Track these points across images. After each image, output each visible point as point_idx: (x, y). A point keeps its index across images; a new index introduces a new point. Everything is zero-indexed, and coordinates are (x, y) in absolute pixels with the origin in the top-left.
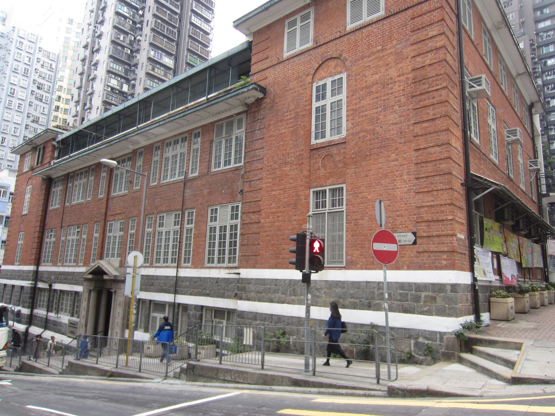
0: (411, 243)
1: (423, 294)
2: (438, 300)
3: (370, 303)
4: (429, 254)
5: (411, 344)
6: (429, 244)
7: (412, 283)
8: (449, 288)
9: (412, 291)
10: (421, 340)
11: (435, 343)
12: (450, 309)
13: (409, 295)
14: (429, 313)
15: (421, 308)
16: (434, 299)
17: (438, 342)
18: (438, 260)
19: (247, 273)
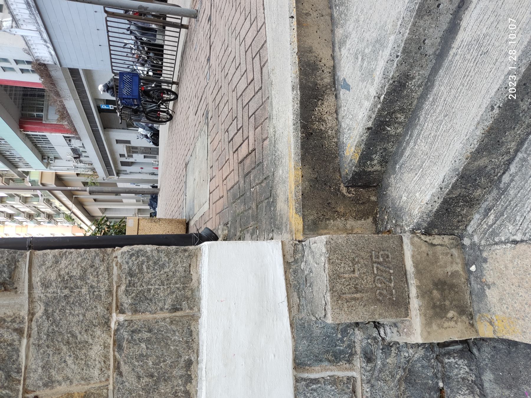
12: (141, 300)
17: (357, 370)
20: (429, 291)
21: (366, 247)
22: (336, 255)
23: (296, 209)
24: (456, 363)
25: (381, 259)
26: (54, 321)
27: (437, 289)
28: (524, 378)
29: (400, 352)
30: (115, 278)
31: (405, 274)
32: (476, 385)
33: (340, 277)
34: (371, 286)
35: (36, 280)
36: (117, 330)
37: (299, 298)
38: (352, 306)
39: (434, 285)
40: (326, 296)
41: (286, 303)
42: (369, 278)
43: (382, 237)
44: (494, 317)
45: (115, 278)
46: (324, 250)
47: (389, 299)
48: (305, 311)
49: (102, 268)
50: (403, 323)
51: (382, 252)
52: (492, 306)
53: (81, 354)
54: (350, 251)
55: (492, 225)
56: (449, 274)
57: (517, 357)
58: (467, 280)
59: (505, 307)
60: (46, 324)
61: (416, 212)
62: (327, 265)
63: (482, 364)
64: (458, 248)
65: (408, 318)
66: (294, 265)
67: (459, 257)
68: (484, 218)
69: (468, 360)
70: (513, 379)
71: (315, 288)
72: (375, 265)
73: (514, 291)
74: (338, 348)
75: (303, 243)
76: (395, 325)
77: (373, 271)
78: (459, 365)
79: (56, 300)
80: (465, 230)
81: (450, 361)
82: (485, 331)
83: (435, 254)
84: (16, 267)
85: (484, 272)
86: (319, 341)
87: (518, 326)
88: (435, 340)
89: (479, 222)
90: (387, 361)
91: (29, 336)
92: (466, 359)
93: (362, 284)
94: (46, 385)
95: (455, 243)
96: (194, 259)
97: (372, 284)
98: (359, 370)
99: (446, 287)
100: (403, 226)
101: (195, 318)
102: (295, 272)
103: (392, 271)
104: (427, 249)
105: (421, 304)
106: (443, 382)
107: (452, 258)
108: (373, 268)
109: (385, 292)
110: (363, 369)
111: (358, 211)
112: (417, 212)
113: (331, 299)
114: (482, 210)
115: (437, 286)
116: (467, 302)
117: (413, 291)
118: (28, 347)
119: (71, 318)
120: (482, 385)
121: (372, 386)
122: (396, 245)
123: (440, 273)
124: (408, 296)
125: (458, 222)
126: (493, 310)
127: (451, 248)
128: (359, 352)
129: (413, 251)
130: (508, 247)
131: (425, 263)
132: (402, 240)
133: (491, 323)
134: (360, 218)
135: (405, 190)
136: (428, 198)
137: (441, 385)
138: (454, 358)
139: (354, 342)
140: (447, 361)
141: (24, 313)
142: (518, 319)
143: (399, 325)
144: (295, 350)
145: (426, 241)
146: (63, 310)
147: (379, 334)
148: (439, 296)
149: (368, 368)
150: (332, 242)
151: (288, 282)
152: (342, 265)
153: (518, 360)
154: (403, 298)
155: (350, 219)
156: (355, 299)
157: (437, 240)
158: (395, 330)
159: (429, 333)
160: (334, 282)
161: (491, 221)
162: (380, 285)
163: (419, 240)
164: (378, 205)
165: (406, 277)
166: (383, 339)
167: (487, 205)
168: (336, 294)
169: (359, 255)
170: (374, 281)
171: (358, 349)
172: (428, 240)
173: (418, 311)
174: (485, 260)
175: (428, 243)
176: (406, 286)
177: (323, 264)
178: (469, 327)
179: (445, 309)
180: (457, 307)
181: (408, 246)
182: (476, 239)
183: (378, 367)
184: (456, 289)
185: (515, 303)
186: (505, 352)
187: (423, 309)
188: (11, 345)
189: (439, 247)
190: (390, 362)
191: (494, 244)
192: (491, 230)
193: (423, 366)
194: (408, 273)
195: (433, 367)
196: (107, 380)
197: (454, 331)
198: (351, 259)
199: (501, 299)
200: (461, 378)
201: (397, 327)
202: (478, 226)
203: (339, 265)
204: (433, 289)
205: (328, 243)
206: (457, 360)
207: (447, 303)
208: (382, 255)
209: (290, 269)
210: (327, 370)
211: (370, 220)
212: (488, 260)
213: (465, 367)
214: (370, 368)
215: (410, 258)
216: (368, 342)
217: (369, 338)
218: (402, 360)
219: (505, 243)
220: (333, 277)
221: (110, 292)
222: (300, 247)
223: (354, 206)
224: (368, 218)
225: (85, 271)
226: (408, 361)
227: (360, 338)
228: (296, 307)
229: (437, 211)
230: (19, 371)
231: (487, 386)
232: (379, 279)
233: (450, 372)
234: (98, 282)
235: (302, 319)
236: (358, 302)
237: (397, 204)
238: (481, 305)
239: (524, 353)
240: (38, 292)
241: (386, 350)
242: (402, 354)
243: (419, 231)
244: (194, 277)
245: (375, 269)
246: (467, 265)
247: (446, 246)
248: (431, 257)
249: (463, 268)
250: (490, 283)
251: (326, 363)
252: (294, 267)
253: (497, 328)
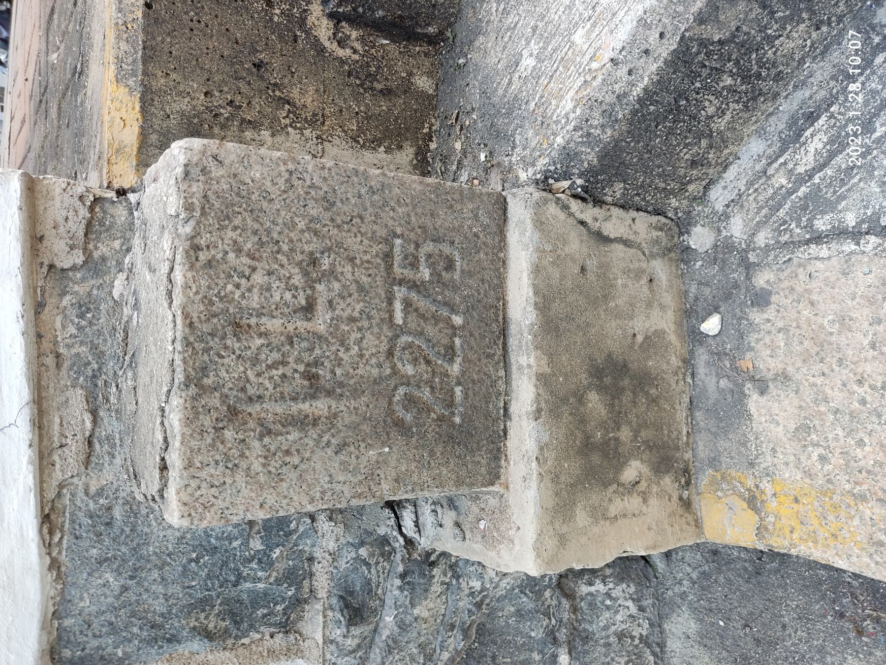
20: (574, 394)
21: (369, 218)
22: (230, 234)
23: (119, 61)
24: (608, 595)
25: (425, 273)
27: (601, 389)
28: (793, 644)
29: (458, 578)
31: (504, 332)
32: (649, 646)
33: (238, 328)
34: (375, 372)
37: (94, 413)
38: (287, 452)
39: (591, 375)
40: (167, 409)
42: (370, 340)
43: (436, 188)
44: (766, 485)
47: (441, 419)
48: (118, 461)
50: (477, 498)
51: (429, 247)
52: (766, 448)
54: (301, 225)
55: (810, 175)
56: (640, 338)
57: (779, 586)
58: (685, 361)
59: (815, 457)
61: (567, 104)
62: (178, 277)
63: (670, 593)
64: (670, 259)
65: (495, 488)
66: (83, 279)
67: (671, 287)
68: (782, 151)
69: (639, 584)
70: (758, 641)
71: (142, 371)
72: (400, 292)
73: (863, 402)
74: (248, 585)
75: (132, 197)
76: (452, 504)
77: (391, 313)
78: (615, 600)
80: (702, 198)
81: (592, 589)
82: (728, 524)
83: (604, 267)
85: (753, 337)
86: (174, 571)
87: (856, 522)
88: (579, 561)
89: (758, 167)
90: (416, 612)
92: (633, 580)
93: (339, 362)
95: (664, 241)
97: (380, 366)
98: (316, 653)
99: (626, 382)
100: (510, 170)
103: (458, 320)
104: (585, 250)
105: (546, 438)
106: (570, 653)
107: (651, 290)
108: (390, 302)
109: (426, 394)
110: (333, 647)
111: (368, 118)
112: (570, 105)
113: (188, 421)
114: (778, 124)
115: (600, 378)
116: (680, 433)
117: (524, 394)
120: (662, 645)
122: (485, 228)
123: (613, 334)
124: (506, 409)
125: (694, 164)
126: (766, 461)
127: (653, 256)
128: (322, 594)
129: (540, 251)
130: (870, 247)
131: (571, 298)
132: (505, 210)
133: (753, 502)
134: (374, 144)
135: (535, 29)
136: (623, 34)
138: (604, 582)
139: (311, 559)
140: (584, 589)
142: (863, 498)
143: (464, 503)
144: (56, 614)
145: (582, 223)
147: (400, 527)
148: (604, 412)
149: (351, 643)
150: (217, 172)
151: (46, 345)
152: (259, 278)
153: (780, 593)
154: (487, 415)
155: (336, 141)
156: (302, 422)
157: (616, 223)
158: (448, 518)
159: (563, 540)
160: (207, 350)
161: (810, 158)
162: (409, 370)
163: (562, 216)
164: (435, 108)
165: (505, 344)
166: (409, 543)
167: (804, 102)
168: (214, 401)
169: (339, 245)
170: (390, 354)
171: (322, 583)
172: (589, 221)
173: (534, 464)
174: (761, 299)
175: (589, 230)
176: (502, 373)
177: (165, 268)
178: (680, 511)
179: (617, 454)
180: (650, 448)
181: (523, 233)
182: (737, 228)
183: (385, 633)
184: (653, 391)
185: (861, 443)
186: (745, 569)
187: (550, 455)
189: (620, 247)
190: (425, 614)
191: (808, 242)
192: (803, 190)
193: (520, 614)
194: (513, 329)
195: (547, 615)
197: (640, 525)
198: (299, 257)
199: (804, 429)
200: (615, 633)
201: (456, 508)
202: (750, 184)
203: (242, 275)
204: (589, 388)
205: (195, 172)
206: (611, 585)
207: (625, 434)
208: (429, 256)
209: (63, 294)
211: (407, 155)
212: (774, 299)
213: (630, 603)
214: (357, 641)
215: (525, 276)
216: (358, 558)
217: (362, 544)
218: (461, 604)
219: (856, 235)
220: (206, 328)
223: (357, 97)
224: (400, 147)
226: (479, 605)
227: (332, 545)
228: (74, 449)
229: (648, 96)
231: (674, 647)
232: (410, 345)
233: (591, 623)
235: (100, 492)
236: (313, 433)
237: (500, 92)
238: (722, 444)
239: (805, 578)
241: (415, 578)
242: (464, 585)
243: (566, 184)
245: (398, 306)
246: (690, 315)
247: (639, 247)
248: (594, 279)
249: (679, 324)
250: (770, 375)
251: (196, 645)
252: (81, 289)
253: (771, 519)
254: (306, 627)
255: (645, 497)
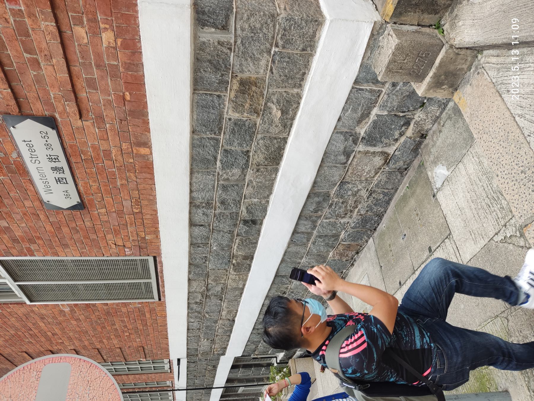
0: (52, 133)
1: (230, 113)
2: (254, 76)
3: (245, 222)
4: (80, 84)
5: (367, 153)
6: (39, 80)
7: (192, 139)
8: (210, 35)
9: (218, 141)
10: (362, 131)
11: (383, 97)
12: (288, 42)
13: (228, 148)
14: (290, 107)
15: (271, 122)
16: (246, 86)
18: (98, 55)
19: (178, 345)
26: (245, 47)
30: (277, 31)
35: (238, 26)
36: (274, 55)
41: (362, 56)
45: (277, 31)
46: (393, 48)
49: (271, 25)
53: (256, 63)
60: (242, 48)
79: (247, 38)
84: (229, 19)
91: (234, 52)
94: (240, 72)
96: (320, 27)
101: (311, 55)
102: (375, 40)
117: (431, 74)
118: (234, 56)
119: (253, 47)
120: (447, 105)
121: (389, 97)
137: (425, 101)
141: (232, 41)
146: (250, 43)
156: (397, 72)
159: (426, 93)
188: (226, 54)
196: (266, 74)
210: (369, 86)
221: (273, 37)
222: (384, 26)
225: (262, 25)
230: (230, 65)
234: (268, 32)
240: (239, 32)
244: (317, 36)
254: (386, 85)
255: (445, 91)
